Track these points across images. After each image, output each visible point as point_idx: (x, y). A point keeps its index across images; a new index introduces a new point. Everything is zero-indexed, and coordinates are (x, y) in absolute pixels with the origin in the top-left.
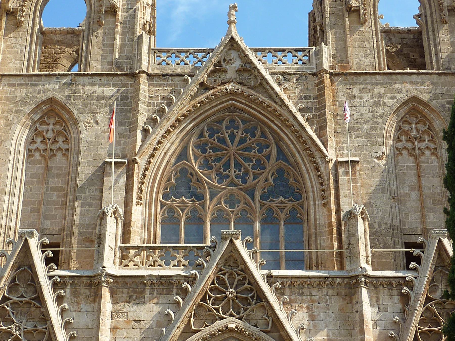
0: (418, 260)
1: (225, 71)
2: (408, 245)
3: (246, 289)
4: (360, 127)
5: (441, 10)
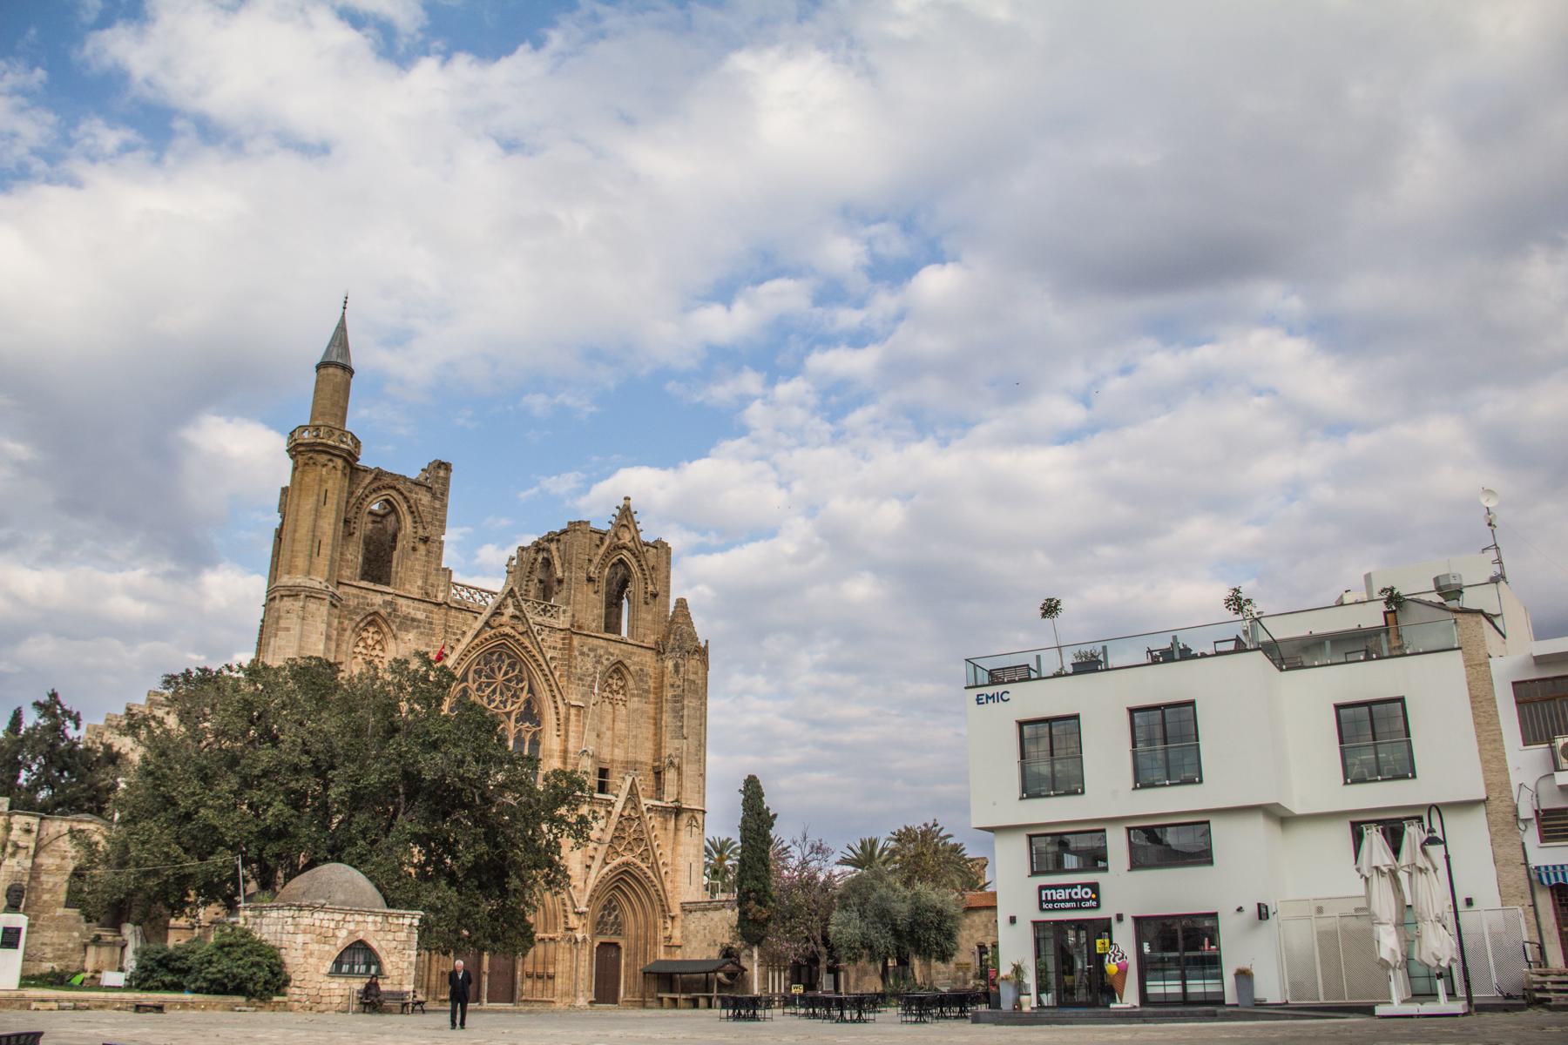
1: (502, 614)
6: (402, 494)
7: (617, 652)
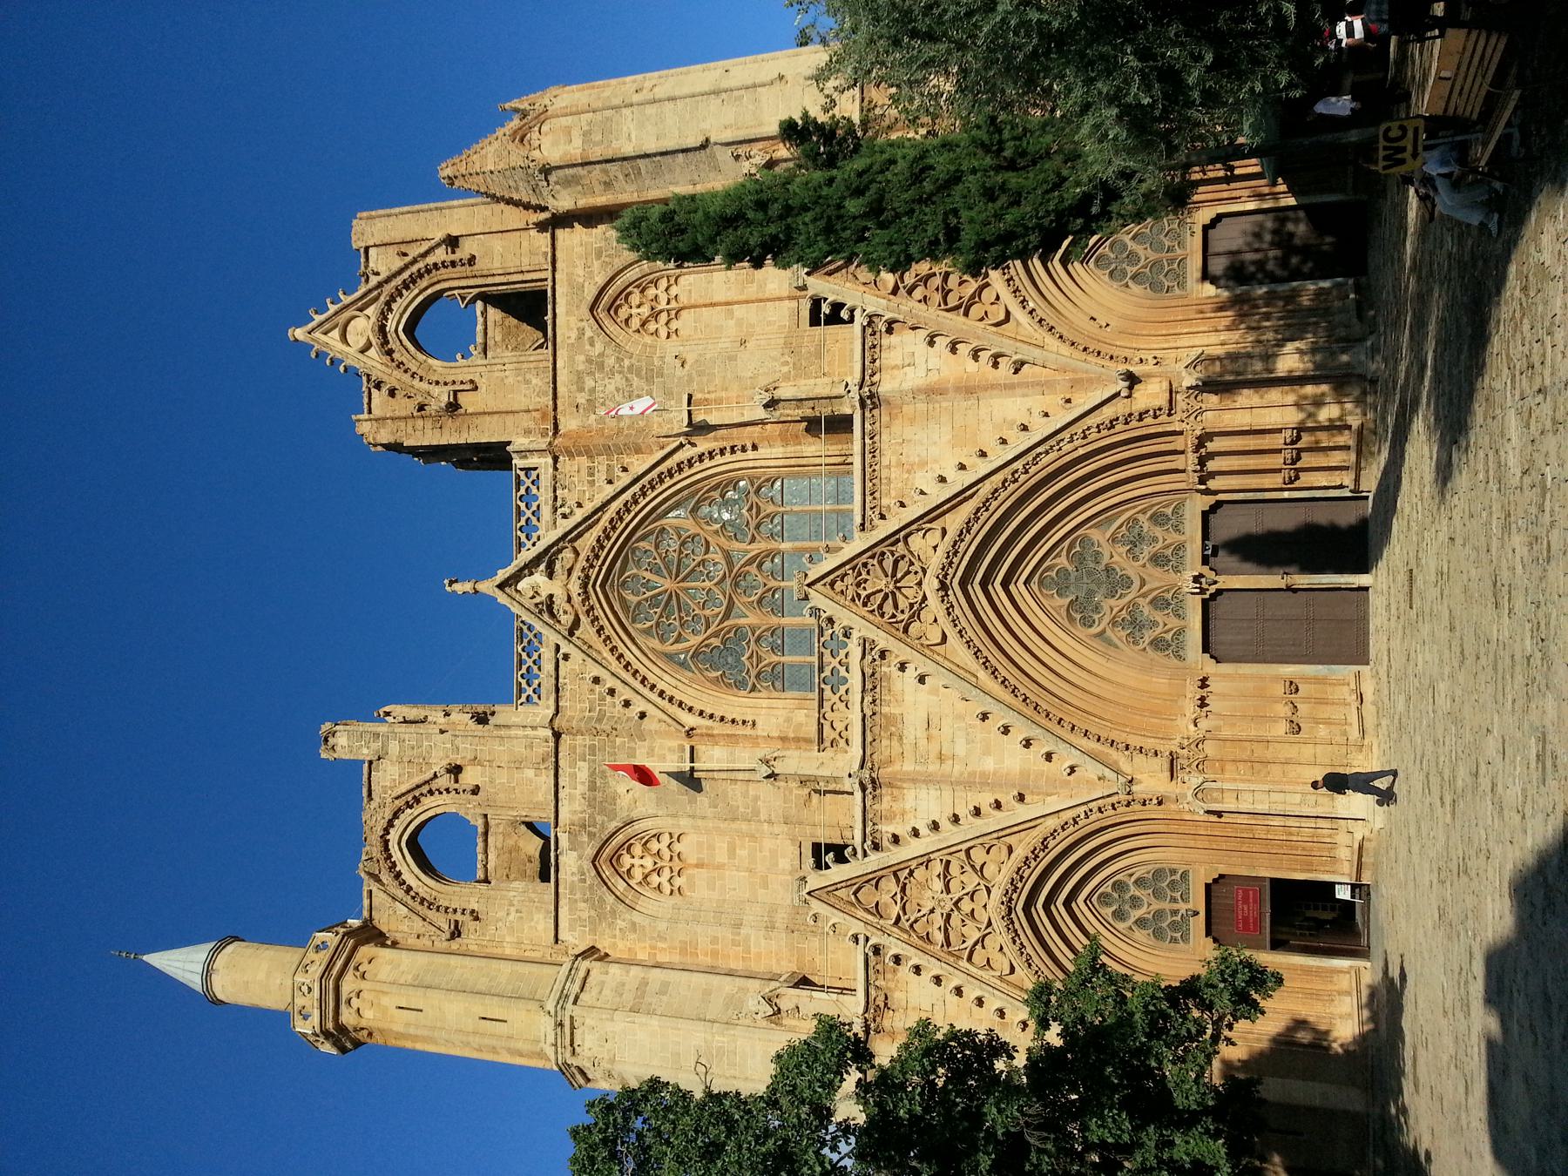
0: (837, 307)
1: (551, 596)
2: (815, 320)
3: (880, 563)
4: (636, 393)
5: (453, 264)
6: (390, 824)
7: (573, 319)
